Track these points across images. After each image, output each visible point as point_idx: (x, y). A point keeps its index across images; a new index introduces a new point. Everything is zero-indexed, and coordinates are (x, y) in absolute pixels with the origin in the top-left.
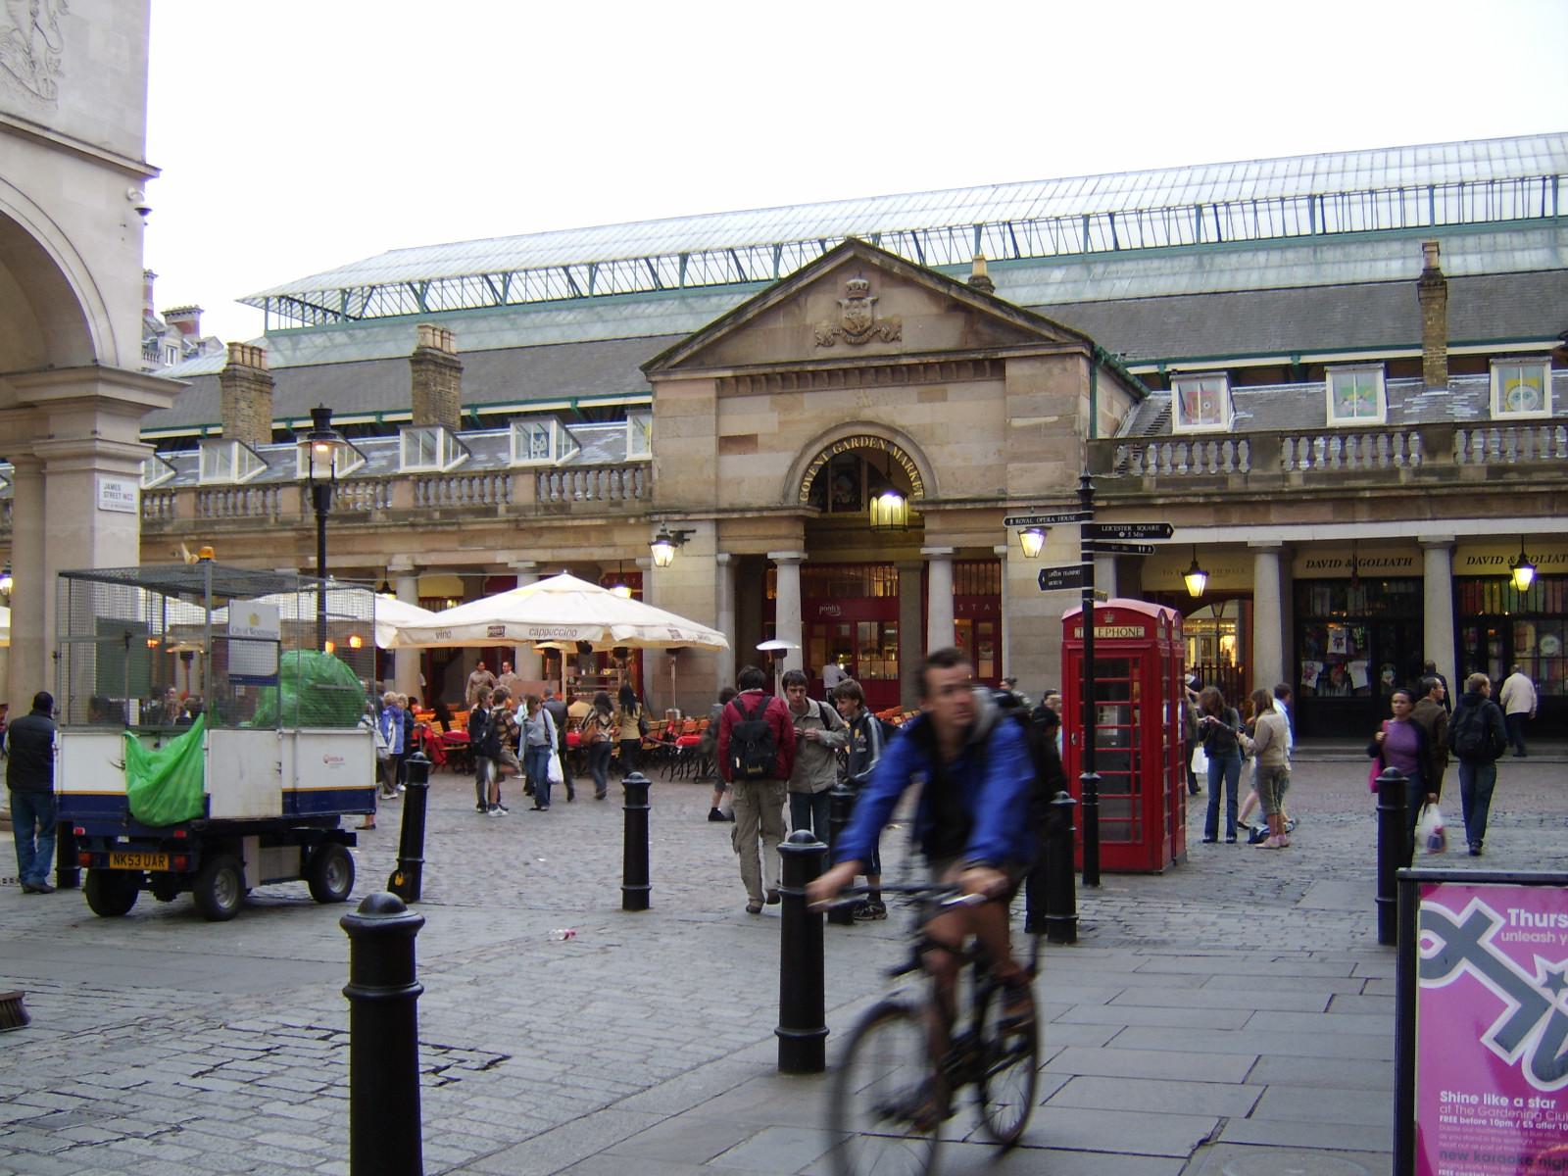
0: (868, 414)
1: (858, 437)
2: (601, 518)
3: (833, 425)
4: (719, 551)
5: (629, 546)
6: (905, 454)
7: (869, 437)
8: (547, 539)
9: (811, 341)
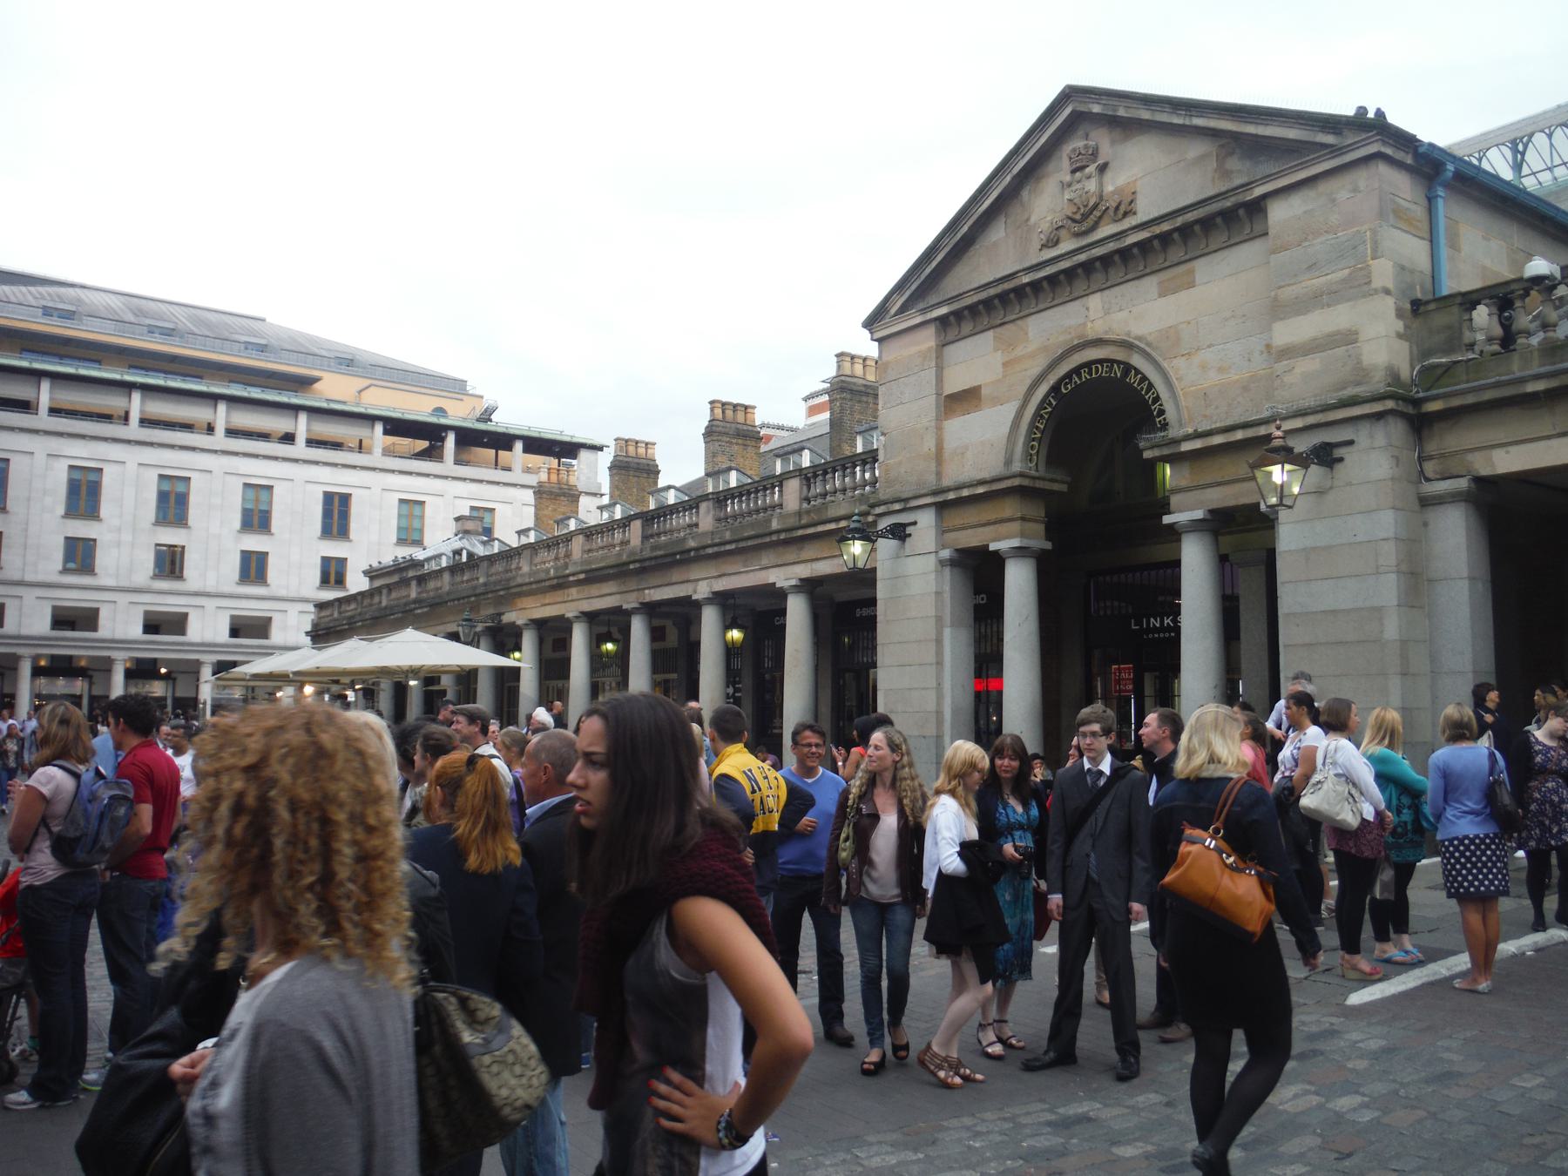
0: (1096, 329)
8: (809, 551)
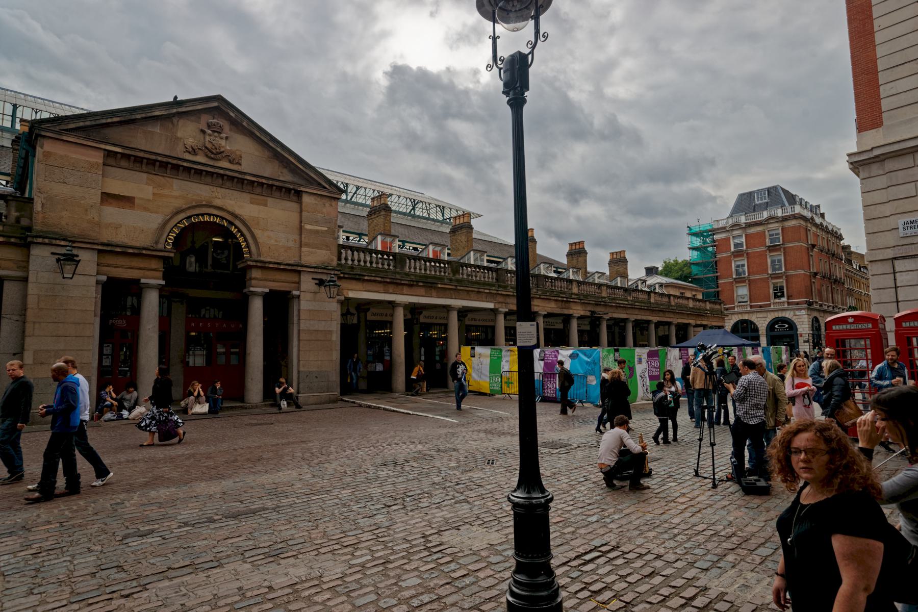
0: (218, 202)
1: (210, 215)
3: (194, 204)
4: (98, 273)
6: (239, 231)
7: (217, 216)
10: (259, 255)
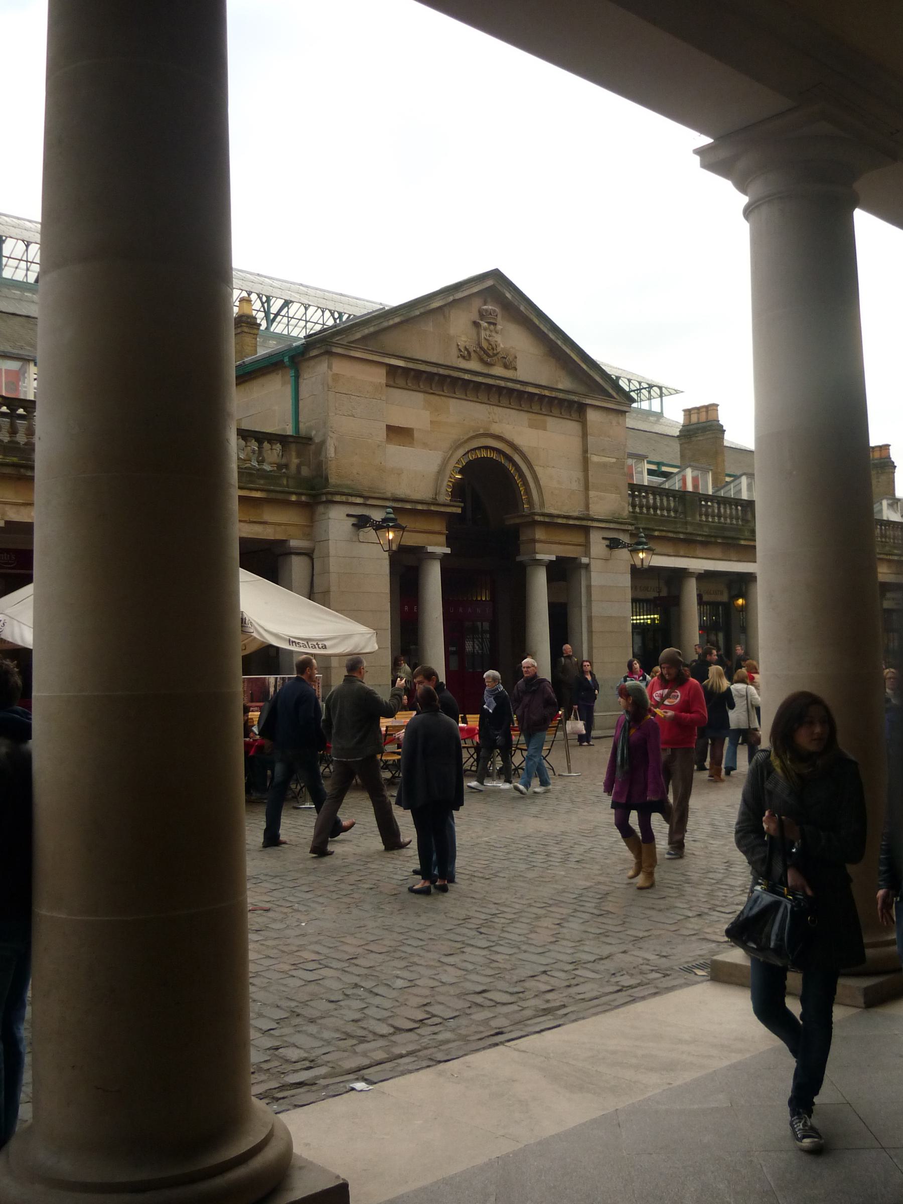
0: (496, 429)
2: (262, 490)
5: (280, 524)
9: (454, 352)
10: (542, 504)
